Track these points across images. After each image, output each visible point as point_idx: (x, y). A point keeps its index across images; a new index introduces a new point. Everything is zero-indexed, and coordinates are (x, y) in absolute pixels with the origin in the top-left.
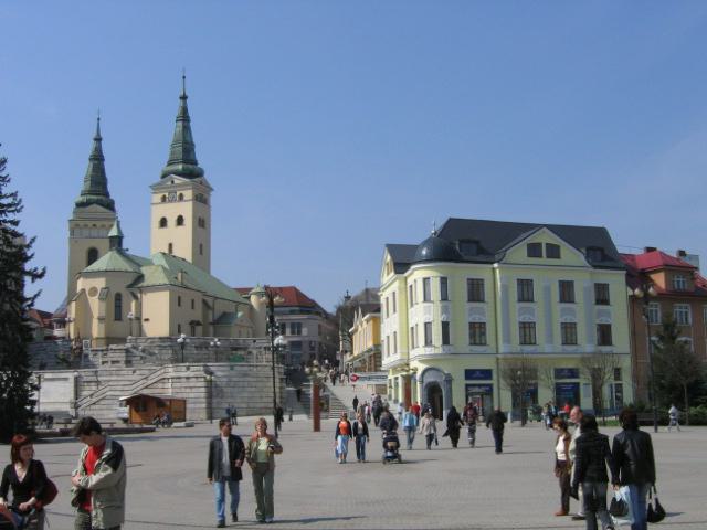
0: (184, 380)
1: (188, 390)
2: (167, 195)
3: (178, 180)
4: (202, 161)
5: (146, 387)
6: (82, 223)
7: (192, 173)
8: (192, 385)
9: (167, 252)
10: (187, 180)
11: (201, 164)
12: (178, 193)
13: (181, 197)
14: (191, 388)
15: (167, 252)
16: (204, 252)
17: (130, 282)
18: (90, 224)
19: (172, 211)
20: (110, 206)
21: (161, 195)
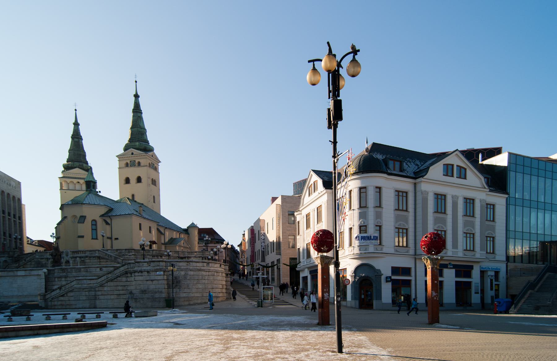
0: (146, 273)
1: (149, 282)
2: (129, 162)
3: (136, 152)
4: (152, 138)
5: (112, 280)
6: (69, 180)
7: (147, 149)
8: (152, 278)
9: (131, 198)
10: (143, 153)
11: (151, 144)
12: (137, 161)
13: (139, 164)
14: (152, 280)
15: (131, 198)
16: (156, 201)
17: (103, 213)
18: (75, 181)
19: (133, 173)
20: (89, 170)
21: (125, 162)
